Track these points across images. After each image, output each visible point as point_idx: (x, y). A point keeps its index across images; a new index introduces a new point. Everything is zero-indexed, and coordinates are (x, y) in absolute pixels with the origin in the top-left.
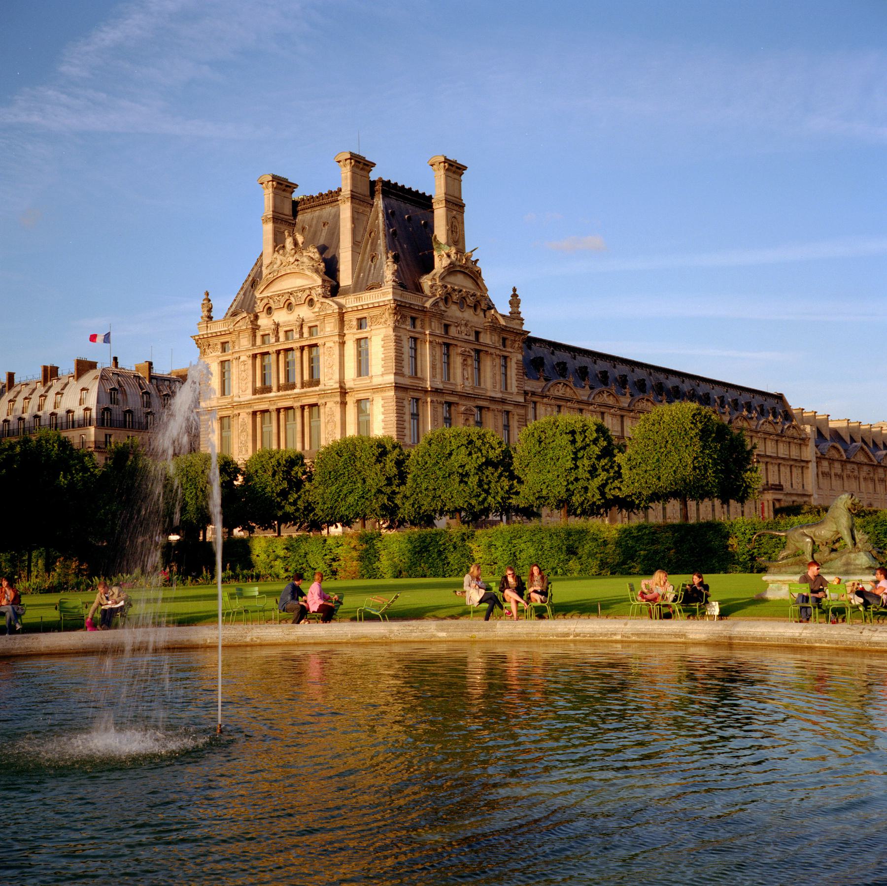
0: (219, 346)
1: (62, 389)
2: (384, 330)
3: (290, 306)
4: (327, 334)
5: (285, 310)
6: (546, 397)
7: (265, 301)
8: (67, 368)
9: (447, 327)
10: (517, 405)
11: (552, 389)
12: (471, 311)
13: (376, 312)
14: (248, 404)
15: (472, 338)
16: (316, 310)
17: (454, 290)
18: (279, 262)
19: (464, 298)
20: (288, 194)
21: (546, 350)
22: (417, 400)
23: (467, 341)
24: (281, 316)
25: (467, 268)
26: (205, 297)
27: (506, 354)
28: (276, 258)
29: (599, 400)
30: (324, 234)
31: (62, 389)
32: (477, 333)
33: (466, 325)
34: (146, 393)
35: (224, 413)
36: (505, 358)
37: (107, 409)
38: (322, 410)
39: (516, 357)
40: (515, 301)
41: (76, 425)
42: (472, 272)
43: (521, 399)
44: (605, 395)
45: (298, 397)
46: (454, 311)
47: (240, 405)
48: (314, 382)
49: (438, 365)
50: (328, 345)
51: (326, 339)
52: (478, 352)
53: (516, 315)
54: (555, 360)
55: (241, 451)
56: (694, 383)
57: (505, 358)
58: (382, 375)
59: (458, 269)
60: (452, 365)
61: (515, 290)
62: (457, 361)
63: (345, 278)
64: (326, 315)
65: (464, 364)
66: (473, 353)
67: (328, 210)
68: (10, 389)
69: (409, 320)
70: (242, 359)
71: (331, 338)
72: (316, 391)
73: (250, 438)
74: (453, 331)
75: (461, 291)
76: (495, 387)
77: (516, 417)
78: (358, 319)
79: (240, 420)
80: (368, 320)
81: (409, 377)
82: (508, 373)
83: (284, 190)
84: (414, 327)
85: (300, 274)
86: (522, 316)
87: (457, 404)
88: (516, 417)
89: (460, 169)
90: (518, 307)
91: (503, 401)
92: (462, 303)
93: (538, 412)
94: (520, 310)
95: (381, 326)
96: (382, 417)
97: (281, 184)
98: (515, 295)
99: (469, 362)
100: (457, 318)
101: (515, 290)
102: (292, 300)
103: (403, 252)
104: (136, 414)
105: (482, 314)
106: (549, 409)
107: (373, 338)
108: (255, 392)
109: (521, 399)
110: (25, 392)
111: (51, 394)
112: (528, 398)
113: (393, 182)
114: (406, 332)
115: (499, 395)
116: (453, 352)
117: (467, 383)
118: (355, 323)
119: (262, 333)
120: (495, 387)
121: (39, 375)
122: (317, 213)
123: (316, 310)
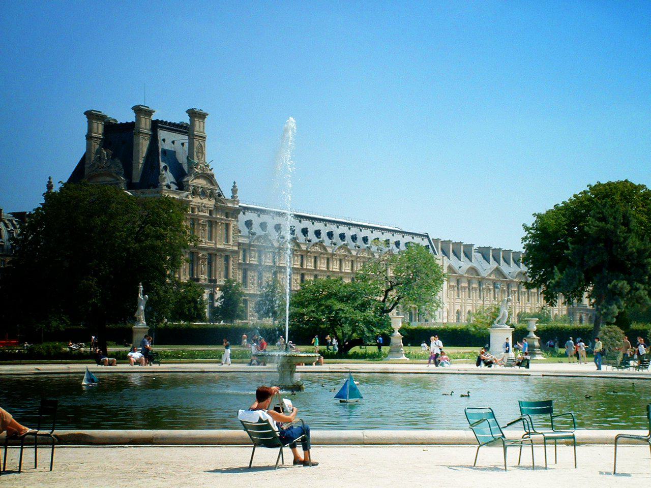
17: (198, 187)
18: (96, 166)
23: (205, 217)
27: (228, 222)
32: (210, 211)
40: (234, 190)
43: (236, 248)
63: (136, 179)
75: (202, 187)
92: (204, 194)
98: (234, 187)
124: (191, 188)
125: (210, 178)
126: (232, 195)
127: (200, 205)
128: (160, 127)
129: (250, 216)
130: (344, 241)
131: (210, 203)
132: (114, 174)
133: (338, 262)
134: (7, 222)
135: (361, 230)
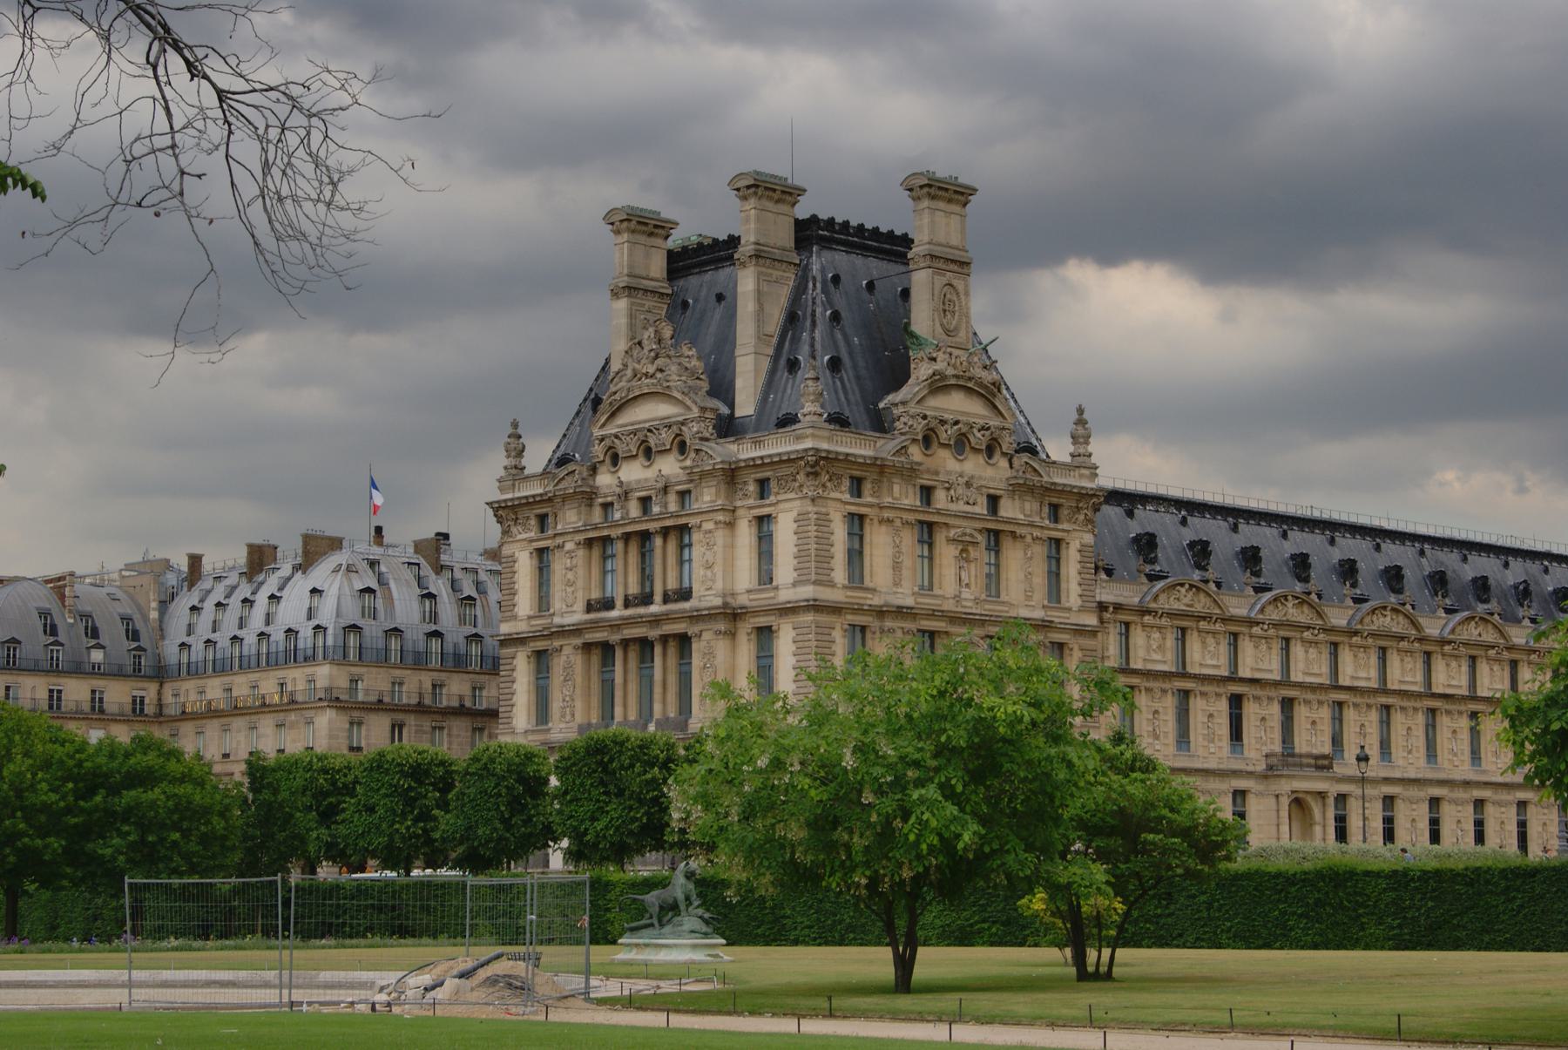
0: (533, 522)
1: (281, 589)
2: (798, 503)
3: (648, 453)
4: (705, 507)
5: (641, 460)
6: (1149, 612)
7: (607, 442)
8: (290, 551)
9: (927, 492)
10: (1080, 631)
11: (1162, 597)
12: (981, 459)
13: (786, 470)
14: (576, 631)
15: (981, 508)
16: (688, 463)
17: (943, 422)
18: (629, 373)
19: (964, 435)
20: (658, 242)
21: (1168, 517)
22: (863, 629)
24: (633, 472)
25: (970, 379)
26: (510, 431)
28: (625, 366)
29: (1274, 614)
30: (717, 317)
31: (281, 589)
32: (993, 501)
33: (968, 485)
34: (431, 596)
35: (540, 645)
36: (1058, 542)
37: (354, 628)
38: (694, 646)
39: (1078, 540)
41: (300, 657)
42: (981, 385)
43: (1091, 620)
44: (1290, 605)
45: (656, 621)
46: (946, 462)
47: (563, 632)
48: (686, 594)
49: (907, 562)
50: (708, 526)
51: (705, 517)
52: (997, 533)
53: (1082, 462)
54: (1188, 535)
55: (563, 716)
56: (1535, 567)
57: (1058, 542)
58: (794, 585)
59: (953, 382)
60: (937, 561)
61: (1080, 411)
62: (947, 554)
63: (745, 406)
64: (703, 475)
65: (964, 556)
66: (980, 538)
67: (723, 273)
68: (191, 585)
69: (846, 483)
70: (569, 546)
71: (711, 515)
72: (685, 611)
73: (578, 691)
74: (940, 499)
75: (957, 423)
76: (1029, 598)
77: (1077, 654)
78: (757, 481)
79: (564, 658)
80: (773, 484)
81: (845, 587)
82: (1063, 571)
83: (651, 234)
84: (859, 496)
85: (663, 395)
86: (1093, 460)
87: (947, 633)
88: (1077, 654)
89: (962, 194)
90: (1087, 443)
91: (1044, 626)
92: (961, 445)
93: (1131, 641)
94: (1090, 449)
95: (792, 495)
96: (792, 661)
97: (646, 224)
98: (1081, 422)
99: (973, 553)
100: (949, 473)
101: (1080, 411)
102: (652, 441)
103: (851, 354)
104: (408, 635)
105: (1004, 463)
106: (1156, 635)
107: (781, 517)
108: (590, 608)
109: (1091, 620)
110: (218, 595)
111: (262, 599)
112: (1107, 615)
113: (839, 220)
114: (839, 505)
115: (1038, 614)
116: (940, 537)
117: (966, 594)
118: (752, 487)
119: (600, 500)
120: (1029, 598)
121: (241, 557)
122: (708, 277)
123: (688, 463)
124: (920, 426)
125: (991, 393)
126: (1071, 449)
127: (953, 478)
128: (823, 238)
129: (1147, 520)
130: (1486, 601)
131: (989, 472)
132: (676, 394)
133: (1465, 668)
134: (458, 574)
135: (1546, 571)
